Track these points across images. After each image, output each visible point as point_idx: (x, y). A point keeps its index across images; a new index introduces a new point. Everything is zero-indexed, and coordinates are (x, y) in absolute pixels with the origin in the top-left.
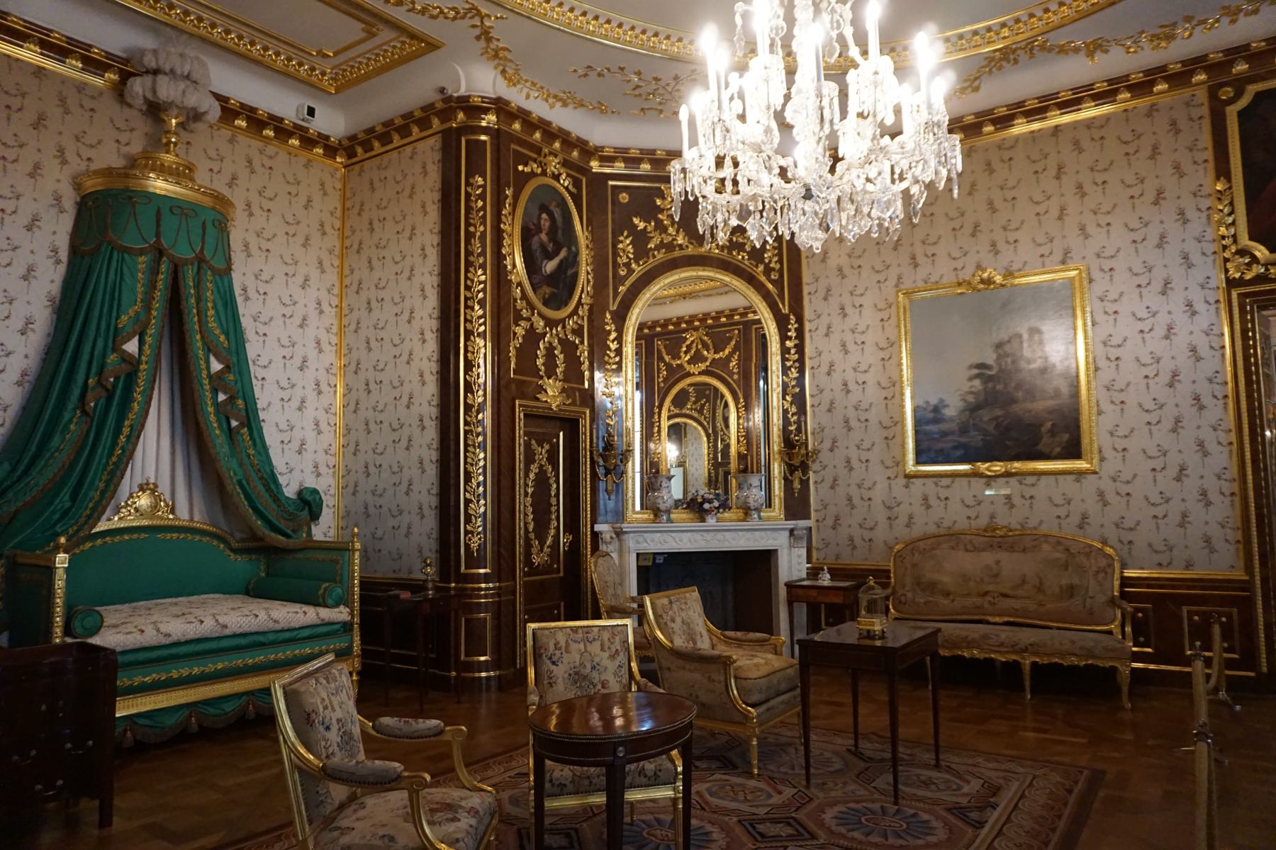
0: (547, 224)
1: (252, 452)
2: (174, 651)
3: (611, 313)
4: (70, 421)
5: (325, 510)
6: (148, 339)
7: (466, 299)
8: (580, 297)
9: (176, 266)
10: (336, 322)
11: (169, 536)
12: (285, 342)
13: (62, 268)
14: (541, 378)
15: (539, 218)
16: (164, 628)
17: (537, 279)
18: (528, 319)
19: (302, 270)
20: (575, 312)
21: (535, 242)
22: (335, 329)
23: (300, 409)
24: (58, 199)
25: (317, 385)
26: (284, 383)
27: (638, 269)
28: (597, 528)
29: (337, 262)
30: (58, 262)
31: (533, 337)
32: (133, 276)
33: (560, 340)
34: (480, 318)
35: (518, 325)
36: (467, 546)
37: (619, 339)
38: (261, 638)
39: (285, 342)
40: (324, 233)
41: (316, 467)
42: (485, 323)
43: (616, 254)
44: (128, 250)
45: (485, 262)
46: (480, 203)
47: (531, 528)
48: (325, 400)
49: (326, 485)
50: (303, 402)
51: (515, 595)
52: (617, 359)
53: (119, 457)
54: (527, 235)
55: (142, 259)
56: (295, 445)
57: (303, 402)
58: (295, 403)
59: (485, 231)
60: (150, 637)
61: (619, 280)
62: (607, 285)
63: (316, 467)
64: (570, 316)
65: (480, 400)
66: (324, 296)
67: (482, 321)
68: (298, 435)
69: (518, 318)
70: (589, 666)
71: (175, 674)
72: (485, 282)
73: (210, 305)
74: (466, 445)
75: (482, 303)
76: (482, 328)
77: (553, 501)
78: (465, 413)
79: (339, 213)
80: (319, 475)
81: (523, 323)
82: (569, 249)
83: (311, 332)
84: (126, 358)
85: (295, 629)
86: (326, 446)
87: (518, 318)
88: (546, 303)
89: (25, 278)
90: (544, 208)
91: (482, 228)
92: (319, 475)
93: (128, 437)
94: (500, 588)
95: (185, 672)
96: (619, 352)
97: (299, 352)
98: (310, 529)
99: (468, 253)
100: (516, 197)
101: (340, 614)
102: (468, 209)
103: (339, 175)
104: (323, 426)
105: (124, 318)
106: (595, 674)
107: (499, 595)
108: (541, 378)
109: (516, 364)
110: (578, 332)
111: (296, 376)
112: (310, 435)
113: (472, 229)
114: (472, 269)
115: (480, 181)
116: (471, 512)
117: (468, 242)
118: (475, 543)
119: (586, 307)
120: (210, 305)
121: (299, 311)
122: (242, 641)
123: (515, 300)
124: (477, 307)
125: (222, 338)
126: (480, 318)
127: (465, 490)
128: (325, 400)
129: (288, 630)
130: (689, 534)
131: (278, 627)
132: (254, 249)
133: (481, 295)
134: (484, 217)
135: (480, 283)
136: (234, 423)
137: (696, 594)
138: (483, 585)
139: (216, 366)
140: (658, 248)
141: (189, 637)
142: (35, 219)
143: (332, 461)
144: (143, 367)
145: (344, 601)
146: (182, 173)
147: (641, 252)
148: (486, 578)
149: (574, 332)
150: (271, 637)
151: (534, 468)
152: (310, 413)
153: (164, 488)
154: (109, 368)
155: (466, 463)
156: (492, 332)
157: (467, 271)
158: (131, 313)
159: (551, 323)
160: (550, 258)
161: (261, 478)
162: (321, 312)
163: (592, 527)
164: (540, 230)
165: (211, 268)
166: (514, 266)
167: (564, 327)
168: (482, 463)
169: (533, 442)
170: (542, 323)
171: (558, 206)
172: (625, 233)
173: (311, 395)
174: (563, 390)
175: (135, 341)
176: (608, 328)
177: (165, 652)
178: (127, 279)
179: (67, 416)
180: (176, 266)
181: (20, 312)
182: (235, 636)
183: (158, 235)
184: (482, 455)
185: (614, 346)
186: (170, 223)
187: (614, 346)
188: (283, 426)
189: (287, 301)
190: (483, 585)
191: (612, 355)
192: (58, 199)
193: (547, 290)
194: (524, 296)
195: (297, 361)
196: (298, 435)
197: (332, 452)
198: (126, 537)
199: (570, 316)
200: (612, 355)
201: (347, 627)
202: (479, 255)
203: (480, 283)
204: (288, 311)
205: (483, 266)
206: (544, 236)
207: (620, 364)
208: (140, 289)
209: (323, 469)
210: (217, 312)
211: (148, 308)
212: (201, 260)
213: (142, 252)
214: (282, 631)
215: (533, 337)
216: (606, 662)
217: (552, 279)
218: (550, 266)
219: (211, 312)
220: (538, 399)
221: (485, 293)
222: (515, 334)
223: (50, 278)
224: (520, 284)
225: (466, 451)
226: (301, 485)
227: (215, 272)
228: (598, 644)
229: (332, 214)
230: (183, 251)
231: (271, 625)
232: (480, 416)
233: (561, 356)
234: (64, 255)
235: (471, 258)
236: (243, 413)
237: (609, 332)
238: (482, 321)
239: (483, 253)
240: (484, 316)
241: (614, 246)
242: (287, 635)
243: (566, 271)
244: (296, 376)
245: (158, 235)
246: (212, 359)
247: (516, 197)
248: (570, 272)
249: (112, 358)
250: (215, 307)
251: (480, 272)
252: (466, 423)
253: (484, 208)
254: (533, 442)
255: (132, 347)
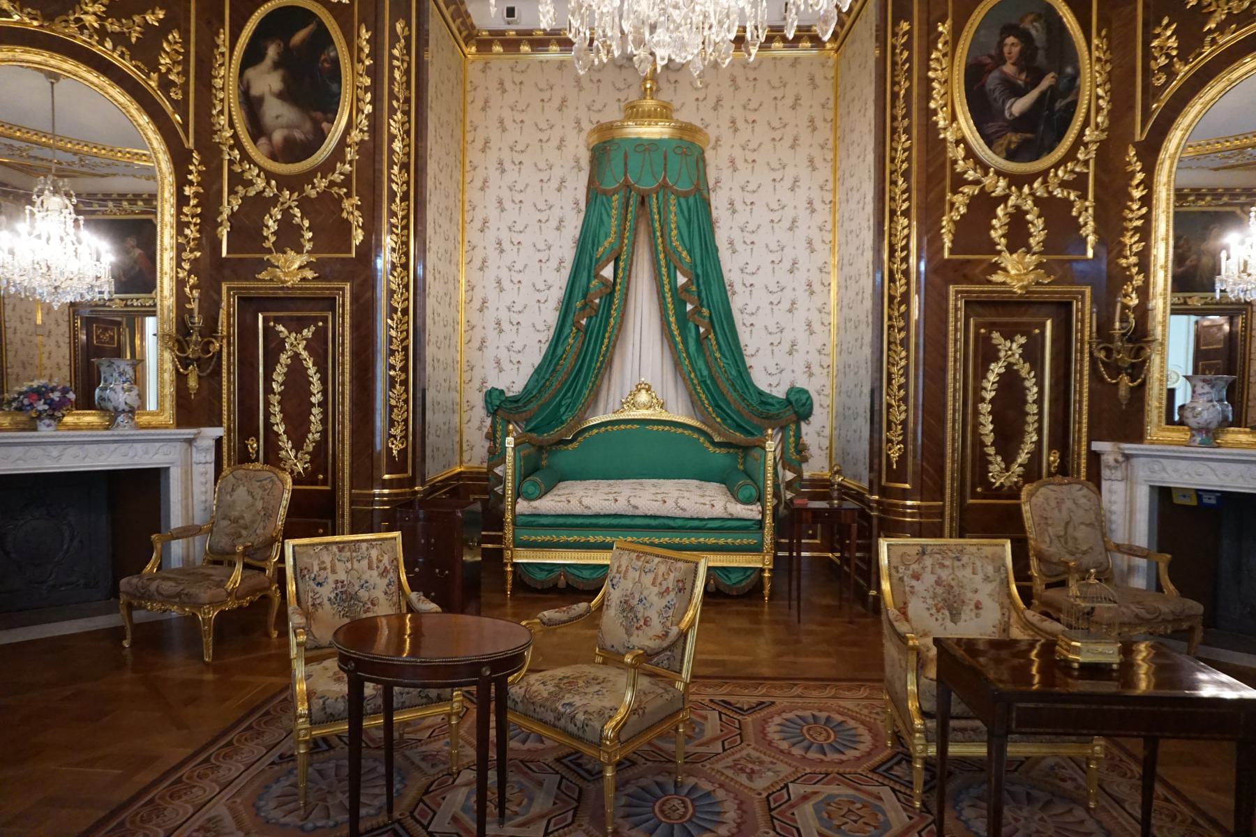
0: (1016, 50)
1: (718, 355)
2: (594, 521)
3: (1136, 145)
4: (567, 337)
5: (817, 410)
6: (621, 264)
7: (892, 173)
8: (1081, 133)
9: (643, 198)
10: (830, 219)
11: (655, 428)
12: (773, 246)
13: (582, 215)
14: (999, 253)
15: (1001, 44)
16: (586, 501)
17: (992, 128)
18: (977, 182)
19: (790, 173)
20: (1071, 156)
21: (992, 81)
22: (829, 226)
23: (790, 311)
24: (577, 161)
25: (810, 285)
26: (773, 287)
27: (1183, 70)
28: (1097, 446)
29: (830, 156)
30: (579, 211)
31: (984, 205)
32: (609, 215)
33: (1037, 201)
34: (903, 192)
35: (955, 191)
36: (888, 455)
37: (1148, 183)
38: (671, 523)
39: (773, 246)
40: (814, 129)
41: (809, 367)
42: (909, 199)
43: (1148, 56)
44: (605, 193)
45: (910, 125)
46: (906, 54)
47: (989, 440)
48: (817, 301)
49: (820, 387)
50: (793, 303)
51: (942, 515)
52: (1144, 210)
53: (602, 362)
54: (975, 76)
55: (616, 196)
56: (786, 346)
57: (793, 303)
58: (786, 305)
59: (911, 86)
60: (621, 506)
61: (1151, 93)
62: (1132, 107)
63: (809, 367)
64: (1056, 166)
65: (903, 289)
66: (816, 195)
67: (905, 196)
68: (788, 336)
69: (959, 181)
70: (637, 597)
71: (591, 539)
72: (909, 149)
73: (673, 226)
74: (889, 343)
75: (906, 175)
76: (905, 206)
77: (1033, 409)
78: (889, 307)
79: (831, 104)
80: (811, 375)
81: (966, 189)
82: (1060, 72)
83: (802, 233)
84: (604, 281)
85: (703, 519)
86: (819, 346)
87: (959, 181)
88: (1011, 156)
89: (558, 229)
90: (1008, 30)
91: (907, 84)
92: (811, 375)
93: (607, 347)
94: (918, 507)
95: (600, 539)
96: (1147, 201)
97: (789, 255)
98: (799, 429)
99: (894, 118)
100: (957, 32)
101: (751, 512)
102: (894, 64)
103: (831, 63)
104: (816, 326)
105: (601, 249)
106: (640, 608)
107: (921, 515)
108: (999, 253)
109: (953, 242)
110: (1078, 183)
111: (785, 278)
112: (802, 336)
113: (896, 88)
114: (896, 137)
115: (905, 26)
116: (891, 418)
117: (893, 106)
118: (895, 455)
119: (1093, 147)
120: (673, 226)
121: (789, 214)
122: (653, 522)
123: (955, 162)
124: (900, 182)
125: (684, 254)
126: (903, 192)
127: (888, 394)
128: (817, 301)
129: (697, 519)
130: (1241, 466)
131: (687, 515)
132: (739, 163)
133: (905, 166)
134: (910, 70)
135: (905, 150)
136: (702, 330)
137: (1008, 545)
138: (377, 491)
139: (681, 280)
140: (1221, 28)
141: (607, 512)
142: (563, 181)
143: (826, 361)
144: (618, 287)
145: (760, 499)
146: (665, 113)
147: (1190, 42)
148: (905, 494)
149: (1063, 184)
150: (679, 523)
151: (997, 369)
152: (801, 315)
153: (656, 387)
154: (592, 290)
155: (888, 363)
156: (918, 208)
157: (892, 140)
158: (606, 244)
159: (1017, 181)
160: (1019, 93)
161: (728, 379)
162: (813, 211)
163: (1089, 445)
164: (1000, 60)
165: (674, 192)
166: (954, 118)
167: (1045, 182)
168: (903, 363)
169: (996, 335)
170: (1002, 183)
171: (1039, 17)
172: (1165, 21)
173: (802, 296)
174: (1039, 266)
175: (611, 267)
176: (1130, 169)
177: (587, 521)
178: (605, 217)
179: (566, 331)
180: (643, 198)
181: (556, 253)
182: (646, 516)
183: (625, 175)
184: (904, 354)
185: (1137, 194)
186: (634, 161)
187: (1137, 194)
188: (773, 328)
189: (775, 206)
190: (909, 503)
191: (1135, 207)
192: (577, 161)
193: (1015, 138)
194: (970, 154)
195: (787, 265)
196: (788, 336)
197: (828, 350)
198: (623, 427)
199: (1056, 166)
200: (1135, 207)
201: (761, 524)
202: (903, 118)
203: (905, 150)
204: (776, 216)
205: (907, 131)
206: (1009, 68)
207: (1147, 218)
208: (614, 222)
209: (816, 369)
210: (680, 233)
211: (622, 238)
212: (664, 186)
213: (615, 192)
214: (692, 519)
215: (984, 205)
216: (654, 599)
217: (1021, 123)
218: (1019, 106)
219: (674, 232)
220: (990, 282)
221: (910, 164)
222: (952, 204)
223: (574, 225)
224: (961, 140)
225: (889, 349)
226: (792, 383)
227: (678, 194)
228: (366, 561)
229: (823, 106)
230: (648, 184)
231: (678, 513)
232: (903, 308)
233: (1040, 223)
234: (583, 206)
235: (895, 124)
236: (707, 320)
237: (1133, 174)
238: (905, 196)
239: (907, 115)
240: (907, 190)
241: (1146, 44)
242: (696, 523)
243: (1053, 100)
244: (785, 278)
245: (625, 175)
246: (678, 274)
247: (957, 32)
248: (1059, 105)
249: (594, 282)
250: (678, 228)
251: (904, 138)
252: (890, 318)
253: (909, 59)
254: (996, 335)
255: (608, 272)
